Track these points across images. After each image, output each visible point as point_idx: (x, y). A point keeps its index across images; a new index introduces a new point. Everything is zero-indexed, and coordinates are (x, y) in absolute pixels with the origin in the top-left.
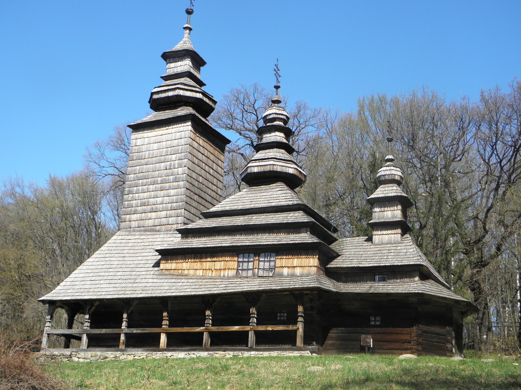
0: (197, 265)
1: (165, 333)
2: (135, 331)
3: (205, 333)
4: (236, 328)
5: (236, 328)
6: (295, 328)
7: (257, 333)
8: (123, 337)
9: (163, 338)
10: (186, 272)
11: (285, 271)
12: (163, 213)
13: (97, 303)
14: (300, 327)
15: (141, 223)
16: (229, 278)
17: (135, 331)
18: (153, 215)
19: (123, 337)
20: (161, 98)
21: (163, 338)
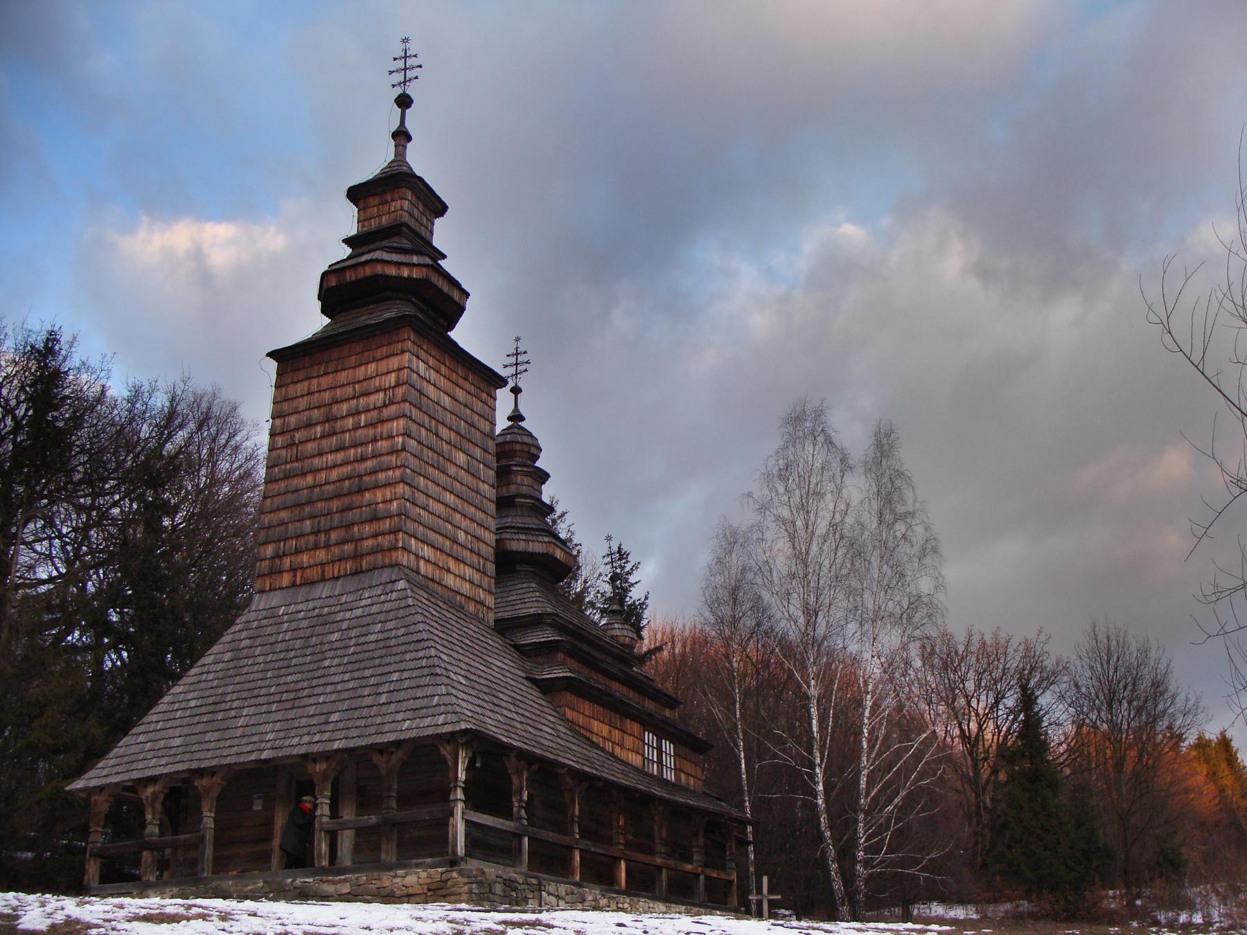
3: (664, 871)
20: (440, 291)
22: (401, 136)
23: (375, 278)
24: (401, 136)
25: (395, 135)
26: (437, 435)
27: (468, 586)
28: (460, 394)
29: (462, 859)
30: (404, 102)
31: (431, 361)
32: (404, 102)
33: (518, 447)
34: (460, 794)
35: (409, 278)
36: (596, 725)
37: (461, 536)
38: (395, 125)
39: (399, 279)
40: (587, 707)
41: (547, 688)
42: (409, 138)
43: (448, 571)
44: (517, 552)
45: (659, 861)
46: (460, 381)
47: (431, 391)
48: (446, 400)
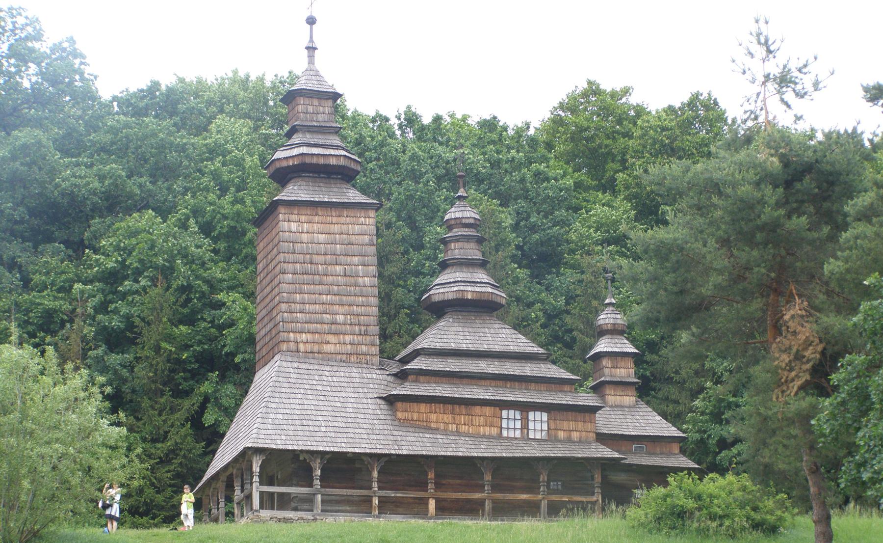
0: (448, 418)
1: (435, 498)
2: (392, 494)
3: (487, 502)
4: (524, 496)
5: (524, 496)
6: (594, 499)
7: (494, 502)
8: (376, 501)
9: (432, 504)
10: (433, 425)
11: (561, 434)
12: (348, 338)
13: (327, 456)
14: (598, 497)
15: (316, 348)
16: (490, 437)
17: (392, 494)
18: (331, 338)
19: (376, 501)
21: (432, 504)
22: (311, 49)
23: (278, 170)
24: (311, 49)
25: (307, 48)
26: (311, 263)
27: (349, 347)
28: (336, 228)
29: (256, 511)
30: (311, 21)
31: (303, 218)
32: (311, 21)
33: (453, 222)
34: (256, 479)
35: (294, 165)
36: (433, 417)
37: (340, 318)
38: (306, 42)
39: (289, 167)
40: (423, 407)
41: (391, 401)
42: (316, 49)
43: (328, 343)
44: (439, 302)
45: (478, 496)
46: (335, 220)
47: (305, 237)
48: (322, 238)
